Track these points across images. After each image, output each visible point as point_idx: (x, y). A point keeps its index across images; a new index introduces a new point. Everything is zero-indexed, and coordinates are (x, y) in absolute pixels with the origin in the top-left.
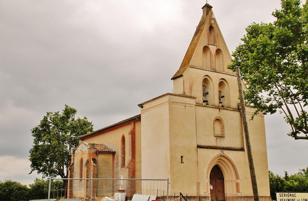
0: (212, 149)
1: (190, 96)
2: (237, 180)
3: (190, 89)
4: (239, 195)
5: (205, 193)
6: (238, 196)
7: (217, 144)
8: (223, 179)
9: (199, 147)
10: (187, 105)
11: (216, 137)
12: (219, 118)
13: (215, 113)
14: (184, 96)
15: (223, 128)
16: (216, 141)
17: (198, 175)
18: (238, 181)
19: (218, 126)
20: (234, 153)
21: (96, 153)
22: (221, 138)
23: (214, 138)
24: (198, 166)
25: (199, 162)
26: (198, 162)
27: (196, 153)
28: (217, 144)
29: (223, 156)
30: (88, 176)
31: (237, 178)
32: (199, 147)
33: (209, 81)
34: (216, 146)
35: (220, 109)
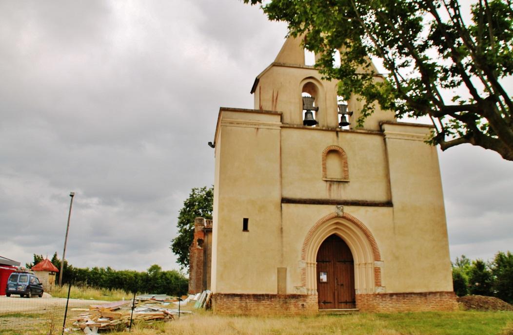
0: (317, 204)
1: (274, 110)
2: (376, 262)
3: (273, 101)
4: (380, 290)
5: (297, 288)
6: (377, 293)
7: (330, 195)
8: (351, 261)
9: (285, 200)
10: (262, 127)
11: (328, 183)
12: (337, 148)
13: (329, 140)
14: (260, 111)
15: (345, 165)
16: (330, 190)
17: (282, 255)
18: (378, 264)
19: (334, 163)
20: (367, 211)
21: (204, 231)
22: (341, 183)
23: (325, 185)
24: (282, 237)
25: (284, 228)
26: (282, 228)
27: (279, 213)
28: (330, 195)
29: (344, 217)
30: (192, 263)
31: (377, 257)
32: (285, 200)
33: (317, 87)
34: (329, 200)
35: (337, 132)
